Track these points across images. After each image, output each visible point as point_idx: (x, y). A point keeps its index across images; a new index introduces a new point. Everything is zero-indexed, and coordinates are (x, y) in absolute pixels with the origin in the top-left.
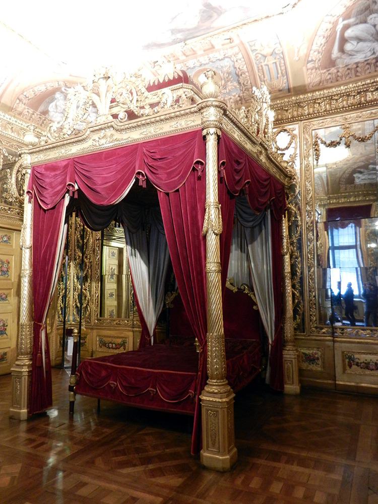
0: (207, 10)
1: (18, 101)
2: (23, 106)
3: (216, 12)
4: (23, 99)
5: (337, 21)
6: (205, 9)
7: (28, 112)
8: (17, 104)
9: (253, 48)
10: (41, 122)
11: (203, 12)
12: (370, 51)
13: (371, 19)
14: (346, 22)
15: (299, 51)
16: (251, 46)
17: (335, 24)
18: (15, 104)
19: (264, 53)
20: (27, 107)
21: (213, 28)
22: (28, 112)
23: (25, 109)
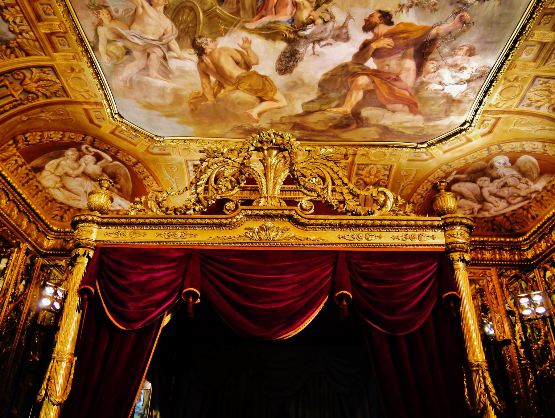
0: (352, 117)
1: (11, 142)
2: (15, 151)
3: (357, 123)
4: (21, 141)
5: (452, 172)
6: (351, 115)
7: (16, 161)
8: (8, 145)
9: (360, 172)
10: (25, 180)
11: (346, 118)
12: (469, 209)
13: (481, 180)
14: (457, 176)
15: (402, 190)
16: (358, 169)
17: (448, 175)
18: (6, 145)
19: (367, 180)
20: (18, 154)
21: (339, 137)
22: (16, 161)
23: (14, 155)
